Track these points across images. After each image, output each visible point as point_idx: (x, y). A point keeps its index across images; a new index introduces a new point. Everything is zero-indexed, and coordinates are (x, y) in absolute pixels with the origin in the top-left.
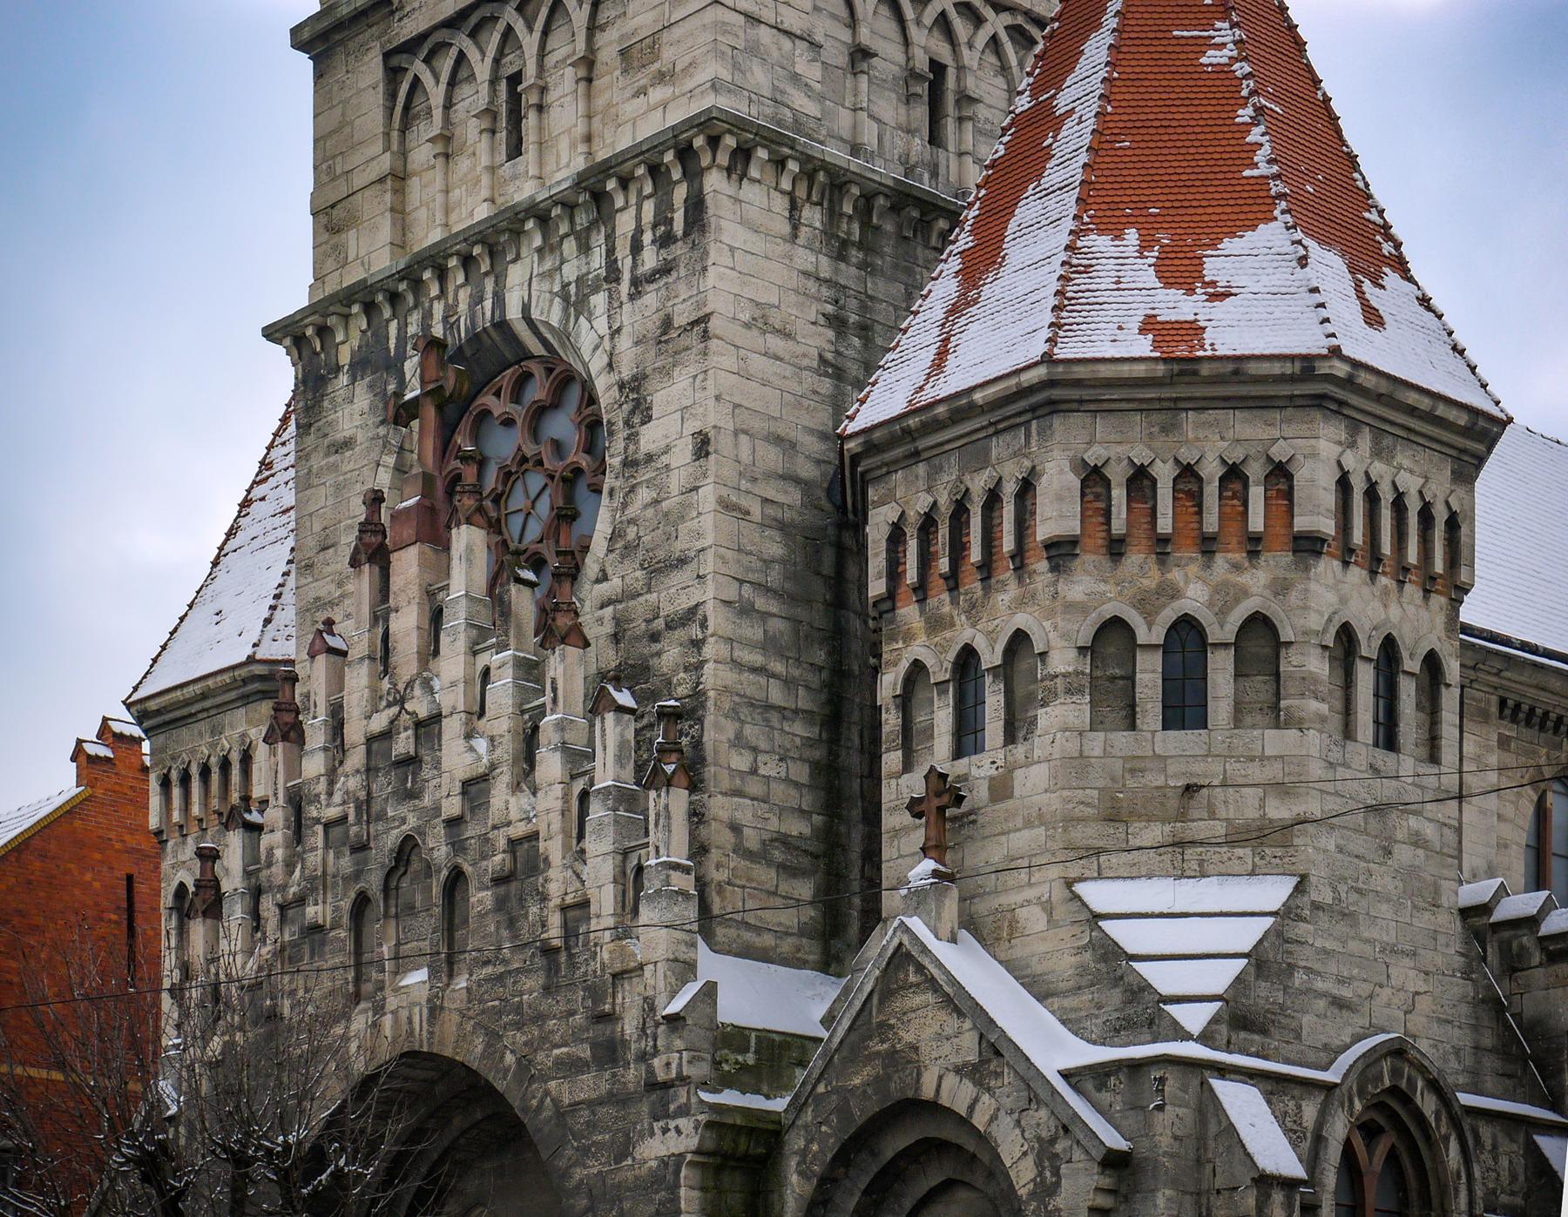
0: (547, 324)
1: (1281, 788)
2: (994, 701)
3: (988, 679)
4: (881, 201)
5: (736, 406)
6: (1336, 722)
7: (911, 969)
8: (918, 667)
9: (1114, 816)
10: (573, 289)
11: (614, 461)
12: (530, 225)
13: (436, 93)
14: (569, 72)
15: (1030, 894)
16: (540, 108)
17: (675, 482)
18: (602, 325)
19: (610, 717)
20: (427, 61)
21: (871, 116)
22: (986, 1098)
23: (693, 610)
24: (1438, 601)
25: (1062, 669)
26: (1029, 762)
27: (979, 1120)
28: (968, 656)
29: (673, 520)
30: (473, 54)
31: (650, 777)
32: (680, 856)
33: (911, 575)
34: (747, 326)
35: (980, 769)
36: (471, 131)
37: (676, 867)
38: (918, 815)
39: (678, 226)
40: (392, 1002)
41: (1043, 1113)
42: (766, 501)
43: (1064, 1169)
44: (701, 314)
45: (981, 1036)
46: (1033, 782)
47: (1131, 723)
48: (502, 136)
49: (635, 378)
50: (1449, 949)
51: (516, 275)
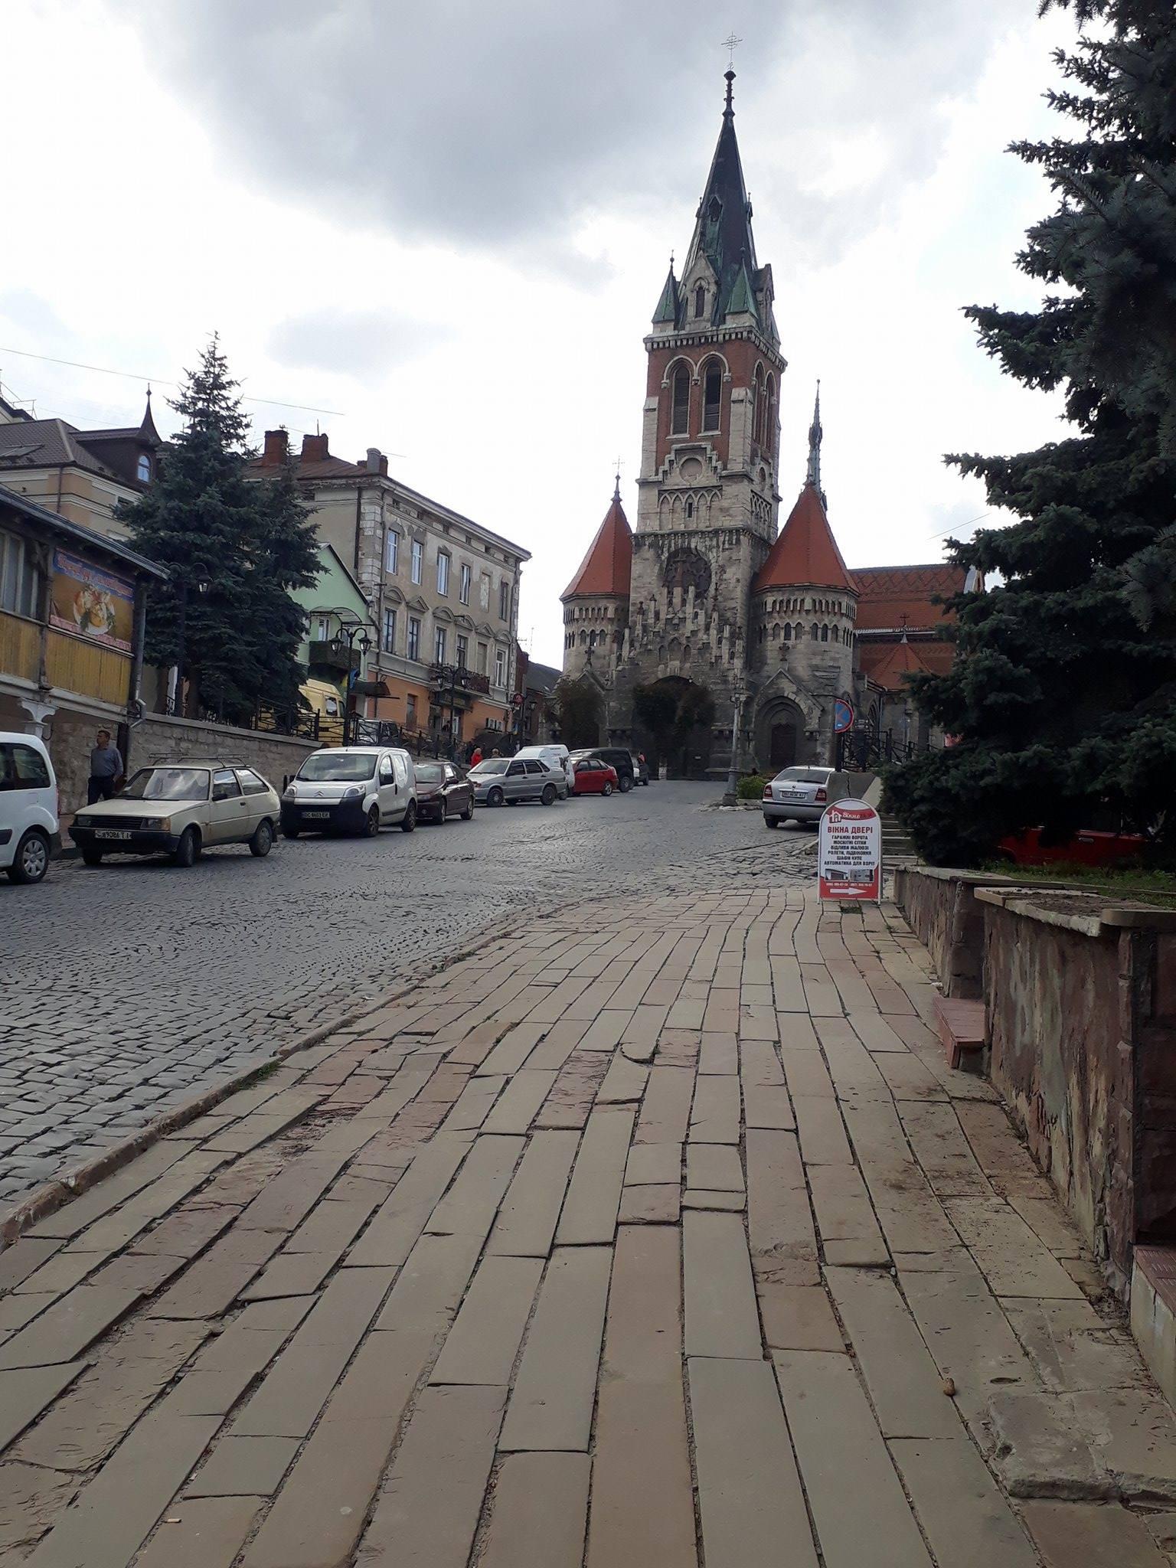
2: (793, 632)
8: (777, 624)
17: (732, 585)
26: (800, 643)
27: (796, 701)
28: (788, 624)
35: (790, 643)
36: (679, 510)
39: (734, 542)
46: (801, 647)
47: (816, 639)
51: (693, 540)
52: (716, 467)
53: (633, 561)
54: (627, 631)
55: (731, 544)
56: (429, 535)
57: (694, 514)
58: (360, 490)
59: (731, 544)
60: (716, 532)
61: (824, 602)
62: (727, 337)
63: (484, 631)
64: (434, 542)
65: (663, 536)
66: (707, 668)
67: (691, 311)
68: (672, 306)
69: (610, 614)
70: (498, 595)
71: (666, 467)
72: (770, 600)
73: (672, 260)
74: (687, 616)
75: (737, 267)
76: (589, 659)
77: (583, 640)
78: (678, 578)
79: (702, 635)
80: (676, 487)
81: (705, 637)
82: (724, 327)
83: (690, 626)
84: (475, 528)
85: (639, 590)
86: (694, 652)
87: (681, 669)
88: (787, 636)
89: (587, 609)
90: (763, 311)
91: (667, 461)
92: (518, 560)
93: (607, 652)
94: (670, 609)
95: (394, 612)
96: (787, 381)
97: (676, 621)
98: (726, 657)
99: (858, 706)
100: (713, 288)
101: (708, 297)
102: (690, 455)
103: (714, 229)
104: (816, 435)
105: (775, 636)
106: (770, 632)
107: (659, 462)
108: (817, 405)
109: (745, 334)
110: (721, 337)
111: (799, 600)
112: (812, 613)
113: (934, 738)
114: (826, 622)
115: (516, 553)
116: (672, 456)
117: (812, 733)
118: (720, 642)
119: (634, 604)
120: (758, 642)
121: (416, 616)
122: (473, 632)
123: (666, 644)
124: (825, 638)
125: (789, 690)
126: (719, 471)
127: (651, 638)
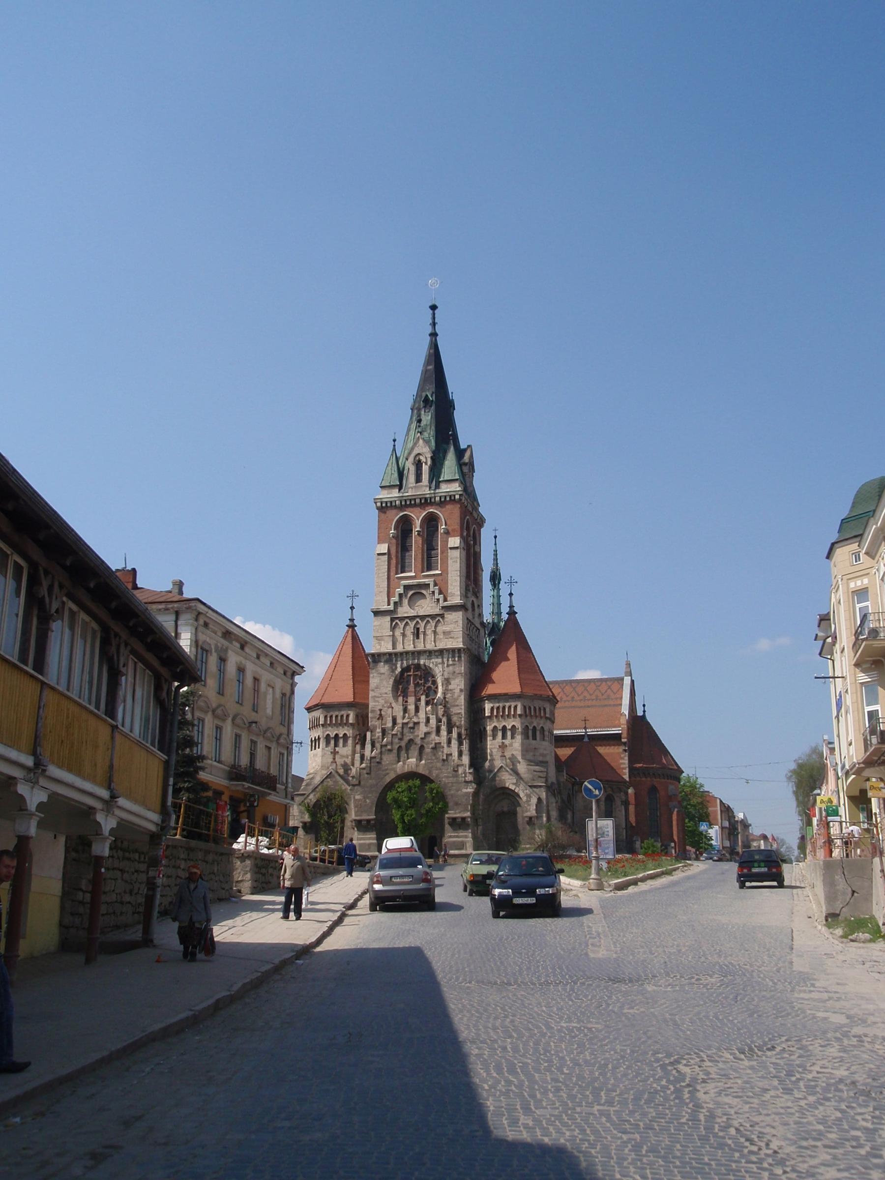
1: (545, 749)
2: (509, 733)
8: (495, 727)
9: (527, 751)
17: (456, 695)
29: (456, 699)
33: (495, 714)
40: (407, 763)
47: (528, 738)
53: (371, 675)
54: (368, 734)
55: (454, 661)
56: (230, 652)
57: (421, 636)
58: (177, 614)
62: (443, 499)
63: (269, 735)
64: (233, 660)
65: (396, 654)
66: (439, 765)
67: (412, 478)
68: (396, 475)
69: (351, 720)
70: (279, 702)
71: (396, 599)
72: (488, 706)
73: (394, 441)
74: (421, 720)
75: (445, 446)
76: (334, 759)
77: (328, 743)
78: (411, 687)
80: (406, 615)
81: (437, 738)
82: (440, 491)
83: (423, 729)
84: (266, 647)
85: (377, 699)
86: (428, 750)
87: (417, 766)
88: (504, 737)
90: (467, 480)
92: (294, 674)
93: (350, 752)
94: (407, 715)
95: (203, 721)
96: (486, 534)
97: (411, 725)
98: (456, 754)
99: (560, 793)
100: (429, 463)
101: (425, 469)
102: (416, 592)
103: (427, 418)
104: (495, 578)
105: (494, 737)
106: (489, 732)
108: (496, 555)
109: (457, 497)
110: (438, 499)
112: (523, 717)
114: (535, 724)
115: (294, 667)
117: (531, 818)
118: (449, 742)
119: (373, 711)
120: (478, 741)
121: (220, 723)
122: (261, 737)
123: (403, 744)
124: (534, 738)
125: (509, 782)
126: (441, 601)
127: (390, 739)
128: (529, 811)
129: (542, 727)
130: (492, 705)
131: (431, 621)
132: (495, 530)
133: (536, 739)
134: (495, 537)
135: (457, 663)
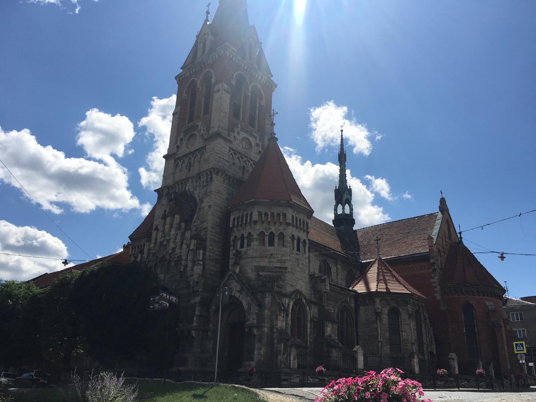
0: (191, 191)
2: (246, 241)
3: (245, 238)
4: (236, 180)
5: (214, 202)
6: (292, 247)
7: (232, 277)
8: (236, 236)
9: (261, 258)
10: (195, 187)
11: (198, 208)
12: (190, 179)
13: (180, 164)
14: (197, 162)
15: (249, 267)
16: (193, 166)
18: (198, 192)
19: (193, 240)
20: (180, 160)
21: (235, 171)
22: (241, 295)
23: (206, 228)
24: (305, 233)
25: (255, 237)
27: (240, 299)
30: (185, 160)
31: (198, 248)
32: (201, 258)
34: (217, 193)
37: (200, 260)
38: (234, 256)
39: (209, 180)
41: (249, 298)
42: (217, 214)
43: (252, 307)
44: (211, 191)
45: (241, 287)
46: (250, 252)
48: (188, 169)
49: (202, 198)
50: (307, 279)
51: (188, 185)
52: (203, 134)
57: (192, 168)
59: (207, 182)
60: (199, 176)
61: (269, 214)
62: (214, 58)
71: (179, 142)
72: (232, 218)
74: (171, 237)
79: (178, 251)
80: (183, 155)
83: (172, 245)
88: (242, 246)
89: (135, 248)
91: (179, 139)
94: (163, 235)
97: (165, 243)
98: (190, 265)
105: (235, 246)
106: (232, 243)
107: (176, 142)
111: (249, 214)
113: (404, 334)
114: (273, 229)
116: (182, 137)
128: (249, 320)
129: (282, 234)
130: (234, 217)
131: (198, 154)
132: (342, 126)
133: (274, 246)
134: (342, 131)
135: (208, 183)
